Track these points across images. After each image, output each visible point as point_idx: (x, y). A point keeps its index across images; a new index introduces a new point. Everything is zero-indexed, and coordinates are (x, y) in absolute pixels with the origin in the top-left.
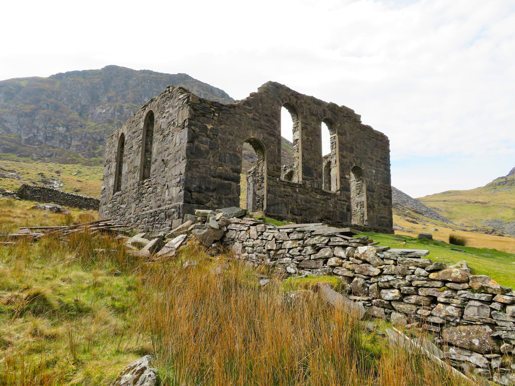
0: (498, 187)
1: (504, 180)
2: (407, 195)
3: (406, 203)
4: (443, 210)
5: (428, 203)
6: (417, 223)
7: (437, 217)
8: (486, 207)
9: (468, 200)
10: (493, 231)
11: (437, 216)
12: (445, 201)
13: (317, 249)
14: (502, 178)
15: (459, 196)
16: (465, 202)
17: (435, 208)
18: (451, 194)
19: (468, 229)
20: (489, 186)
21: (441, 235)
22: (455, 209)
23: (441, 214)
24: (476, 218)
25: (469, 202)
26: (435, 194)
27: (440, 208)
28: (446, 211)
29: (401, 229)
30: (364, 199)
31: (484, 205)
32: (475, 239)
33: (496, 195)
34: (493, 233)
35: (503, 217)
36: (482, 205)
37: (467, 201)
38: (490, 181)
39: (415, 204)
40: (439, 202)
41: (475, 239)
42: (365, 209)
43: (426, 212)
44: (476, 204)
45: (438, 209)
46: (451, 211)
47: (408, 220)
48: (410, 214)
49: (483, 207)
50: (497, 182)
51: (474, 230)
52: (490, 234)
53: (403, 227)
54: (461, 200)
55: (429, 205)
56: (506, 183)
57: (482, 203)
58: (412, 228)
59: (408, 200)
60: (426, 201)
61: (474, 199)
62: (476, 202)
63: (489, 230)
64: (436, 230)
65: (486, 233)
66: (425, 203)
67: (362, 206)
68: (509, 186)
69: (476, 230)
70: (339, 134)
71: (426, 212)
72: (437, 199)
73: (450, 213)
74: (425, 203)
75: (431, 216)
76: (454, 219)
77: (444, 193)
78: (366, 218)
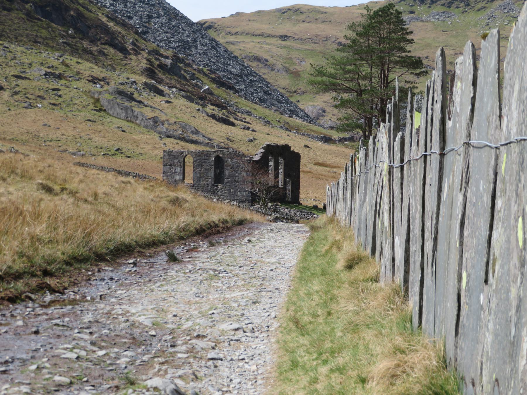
3: (189, 48)
5: (240, 39)
7: (266, 93)
11: (265, 89)
12: (284, 38)
13: (304, 215)
15: (322, 26)
17: (257, 59)
18: (303, 17)
23: (269, 76)
26: (259, 13)
27: (271, 60)
28: (287, 70)
29: (207, 141)
30: (290, 188)
39: (213, 52)
40: (268, 40)
42: (290, 193)
43: (241, 76)
45: (265, 62)
46: (299, 68)
47: (213, 116)
48: (211, 93)
51: (345, 139)
53: (210, 136)
54: (327, 39)
55: (241, 46)
58: (228, 139)
59: (195, 41)
60: (234, 31)
66: (232, 39)
67: (289, 191)
68: (445, 9)
70: (284, 159)
71: (241, 76)
72: (266, 28)
74: (232, 39)
75: (250, 90)
77: (284, 12)
78: (290, 197)
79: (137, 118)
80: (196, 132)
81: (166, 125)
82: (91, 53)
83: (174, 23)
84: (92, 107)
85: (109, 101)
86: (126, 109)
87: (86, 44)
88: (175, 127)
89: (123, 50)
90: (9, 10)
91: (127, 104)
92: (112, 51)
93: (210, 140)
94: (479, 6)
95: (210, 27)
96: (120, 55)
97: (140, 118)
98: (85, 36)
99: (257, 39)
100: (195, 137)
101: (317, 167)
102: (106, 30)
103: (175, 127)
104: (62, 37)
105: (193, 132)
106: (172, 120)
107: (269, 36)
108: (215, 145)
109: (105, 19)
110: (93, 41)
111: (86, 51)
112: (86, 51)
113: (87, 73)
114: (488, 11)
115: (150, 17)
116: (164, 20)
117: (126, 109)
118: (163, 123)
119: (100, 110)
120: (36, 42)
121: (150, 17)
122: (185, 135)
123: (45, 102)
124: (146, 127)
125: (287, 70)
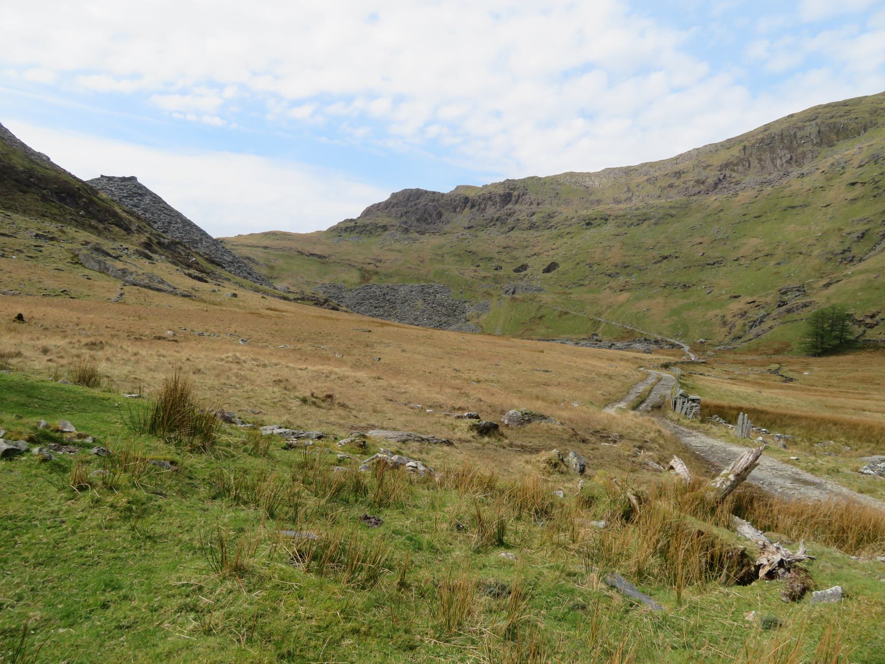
0: (344, 234)
1: (353, 224)
2: (201, 230)
3: (197, 243)
4: (262, 262)
5: (238, 247)
6: (206, 282)
7: (249, 274)
8: (324, 263)
9: (300, 250)
10: (326, 301)
12: (266, 248)
14: (351, 220)
15: (288, 242)
16: (296, 253)
17: (249, 258)
18: (277, 237)
19: (291, 296)
20: (333, 230)
21: (241, 304)
22: (280, 263)
23: (256, 268)
24: (309, 280)
25: (301, 253)
26: (251, 234)
27: (257, 259)
28: (266, 265)
29: (171, 289)
31: (322, 260)
32: (293, 313)
33: (340, 246)
34: (325, 306)
35: (344, 281)
36: (319, 260)
37: (298, 251)
38: (334, 223)
39: (214, 247)
40: (255, 249)
41: (293, 313)
44: (311, 257)
45: (253, 261)
46: (274, 264)
47: (190, 275)
48: (198, 264)
49: (320, 262)
50: (343, 226)
51: (298, 299)
52: (321, 305)
53: (176, 286)
54: (291, 249)
55: (239, 251)
56: (355, 229)
57: (320, 257)
59: (201, 239)
60: (236, 244)
61: (309, 249)
62: (311, 254)
63: (320, 300)
64: (235, 295)
65: (316, 304)
66: (233, 247)
68: (358, 235)
69: (303, 299)
71: (232, 262)
72: (255, 242)
73: (272, 268)
74: (233, 247)
75: (238, 271)
76: (276, 278)
77: (266, 235)
79: (108, 269)
80: (162, 282)
81: (134, 276)
82: (96, 228)
83: (187, 228)
84: (69, 260)
85: (85, 256)
86: (99, 262)
87: (93, 222)
88: (142, 277)
89: (128, 230)
90: (25, 192)
91: (101, 258)
92: (117, 229)
93: (175, 289)
94: (377, 234)
95: (221, 242)
96: (124, 232)
97: (111, 269)
98: (94, 217)
99: (249, 248)
100: (160, 286)
101: (267, 311)
102: (115, 214)
103: (142, 277)
104: (71, 214)
105: (159, 282)
106: (140, 272)
107: (257, 247)
108: (178, 292)
109: (119, 211)
110: (101, 221)
111: (91, 226)
112: (91, 226)
113: (82, 239)
114: (383, 237)
115: (170, 223)
116: (180, 225)
117: (99, 262)
118: (131, 274)
119: (77, 263)
120: (43, 216)
121: (170, 223)
122: (151, 284)
123: (22, 255)
124: (115, 277)
125: (266, 265)
